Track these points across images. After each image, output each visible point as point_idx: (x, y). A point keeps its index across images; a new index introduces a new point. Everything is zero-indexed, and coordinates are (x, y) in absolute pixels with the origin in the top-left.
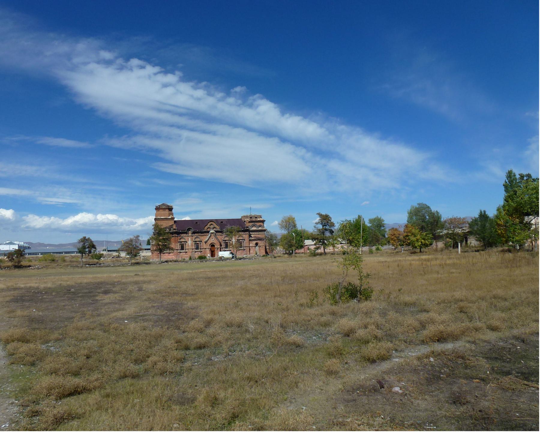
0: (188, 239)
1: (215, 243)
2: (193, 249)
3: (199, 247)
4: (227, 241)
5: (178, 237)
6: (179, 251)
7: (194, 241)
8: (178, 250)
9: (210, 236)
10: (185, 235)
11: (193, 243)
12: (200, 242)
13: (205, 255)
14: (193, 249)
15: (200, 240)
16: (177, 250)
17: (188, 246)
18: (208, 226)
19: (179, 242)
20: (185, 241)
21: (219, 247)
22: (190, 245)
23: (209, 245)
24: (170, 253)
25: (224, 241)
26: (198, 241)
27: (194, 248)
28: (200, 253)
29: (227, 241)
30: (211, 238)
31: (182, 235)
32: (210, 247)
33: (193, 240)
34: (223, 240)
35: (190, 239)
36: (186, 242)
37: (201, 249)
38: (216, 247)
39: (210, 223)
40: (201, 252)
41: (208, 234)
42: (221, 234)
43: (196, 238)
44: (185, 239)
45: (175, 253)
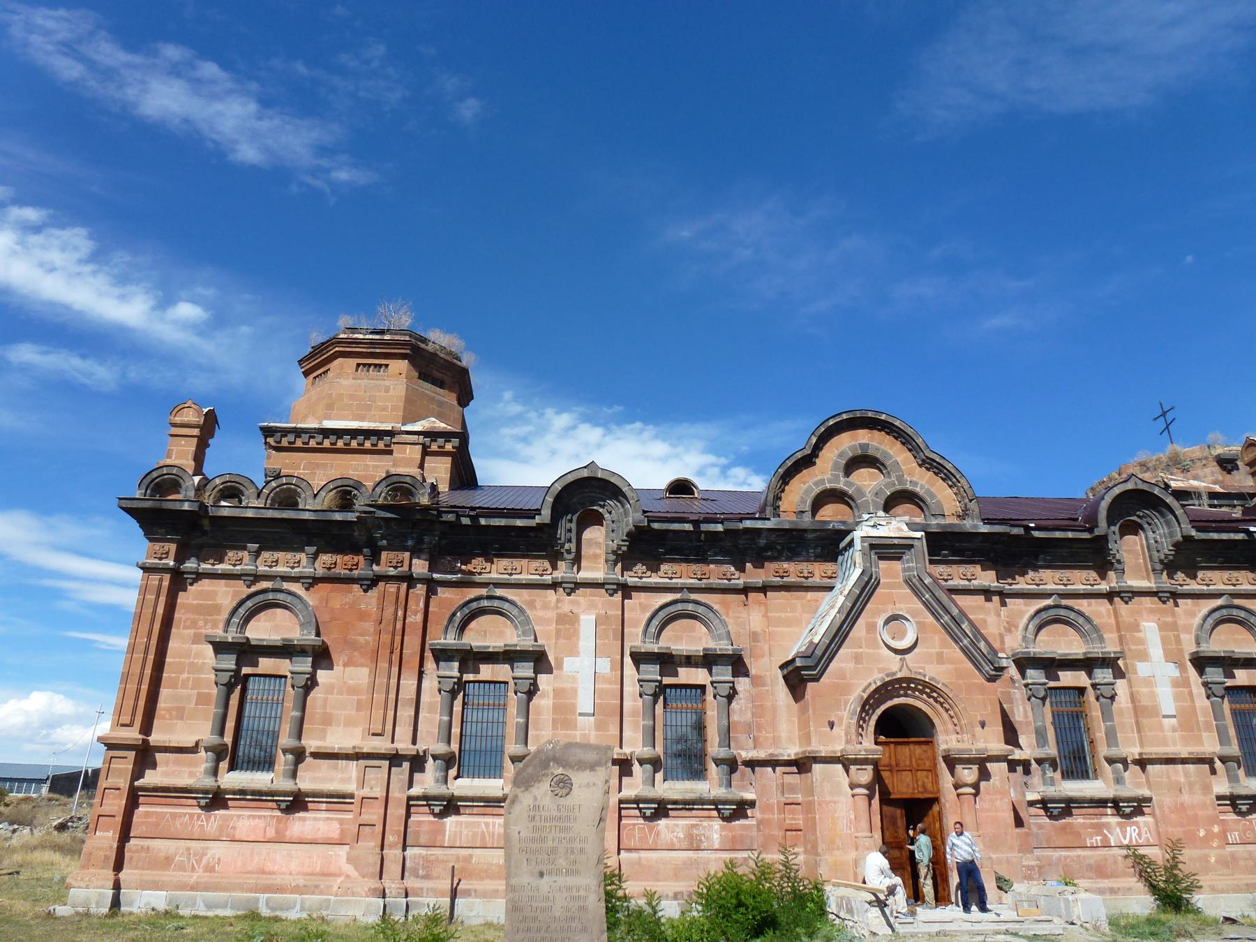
0: (568, 622)
1: (928, 688)
2: (624, 766)
3: (714, 748)
4: (1068, 678)
5: (432, 586)
6: (428, 782)
7: (639, 658)
8: (418, 763)
9: (867, 588)
10: (528, 569)
11: (631, 688)
12: (724, 673)
13: (800, 858)
14: (624, 766)
15: (723, 646)
16: (395, 759)
17: (564, 713)
18: (825, 472)
19: (442, 655)
20: (526, 643)
21: (993, 742)
22: (585, 703)
23: (847, 714)
24: (297, 803)
25: (1035, 675)
26: (689, 661)
27: (635, 745)
28: (714, 830)
29: (1068, 678)
30: (875, 613)
31: (497, 570)
32: (867, 745)
33: (636, 640)
34: (1024, 663)
35: (587, 621)
36: (539, 660)
37: (731, 765)
38: (947, 740)
39: (846, 443)
40: (741, 809)
41: (818, 571)
42: (987, 578)
43: (666, 619)
44: (525, 623)
45: (373, 814)
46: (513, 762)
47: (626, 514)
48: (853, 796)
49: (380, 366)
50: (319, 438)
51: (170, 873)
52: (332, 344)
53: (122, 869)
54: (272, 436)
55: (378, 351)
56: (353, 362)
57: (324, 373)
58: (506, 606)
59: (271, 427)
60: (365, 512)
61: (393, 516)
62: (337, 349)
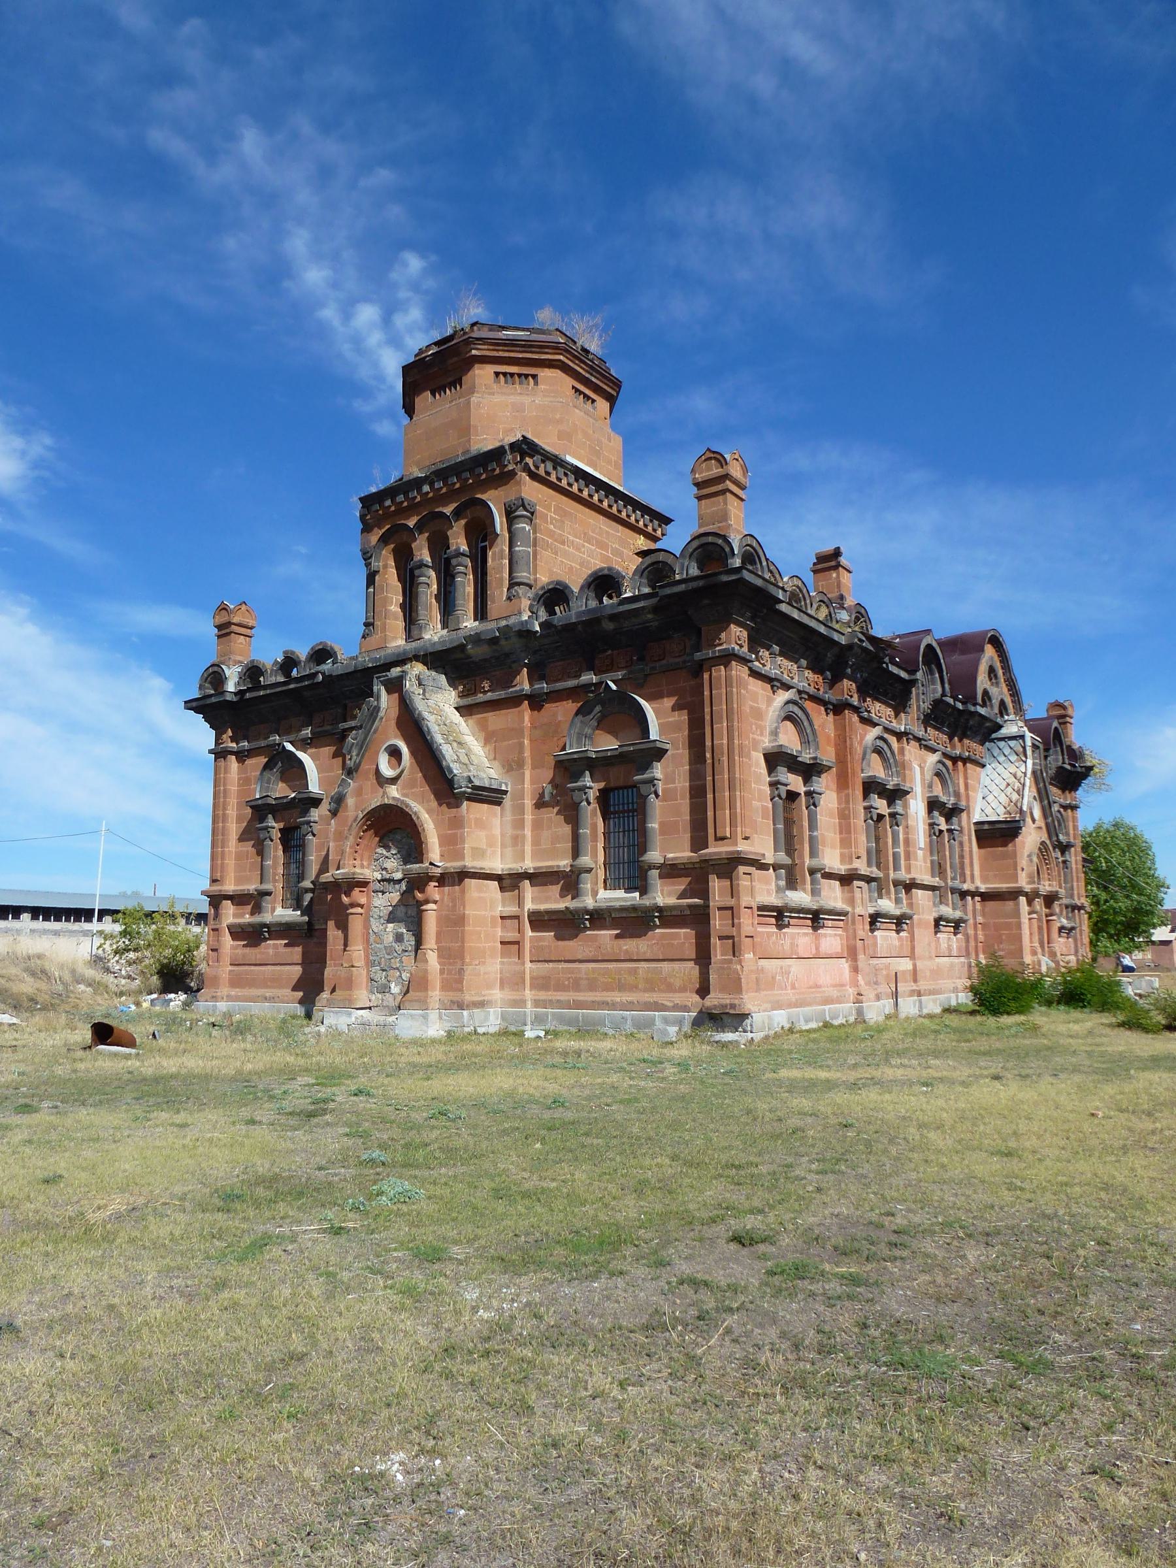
46: (895, 886)
47: (934, 683)
48: (1030, 919)
49: (587, 398)
50: (572, 478)
51: (776, 992)
52: (557, 348)
53: (708, 993)
54: (532, 456)
55: (593, 379)
56: (569, 382)
57: (520, 375)
58: (885, 747)
59: (537, 445)
60: (860, 640)
61: (871, 648)
62: (561, 357)
